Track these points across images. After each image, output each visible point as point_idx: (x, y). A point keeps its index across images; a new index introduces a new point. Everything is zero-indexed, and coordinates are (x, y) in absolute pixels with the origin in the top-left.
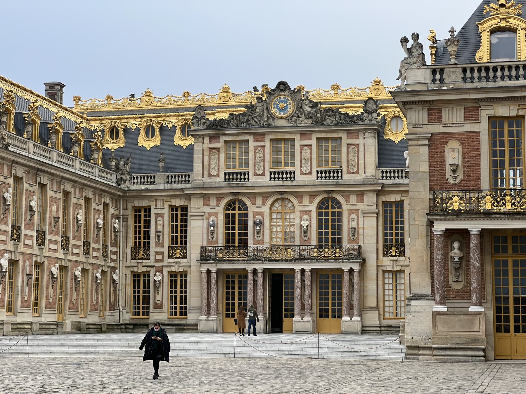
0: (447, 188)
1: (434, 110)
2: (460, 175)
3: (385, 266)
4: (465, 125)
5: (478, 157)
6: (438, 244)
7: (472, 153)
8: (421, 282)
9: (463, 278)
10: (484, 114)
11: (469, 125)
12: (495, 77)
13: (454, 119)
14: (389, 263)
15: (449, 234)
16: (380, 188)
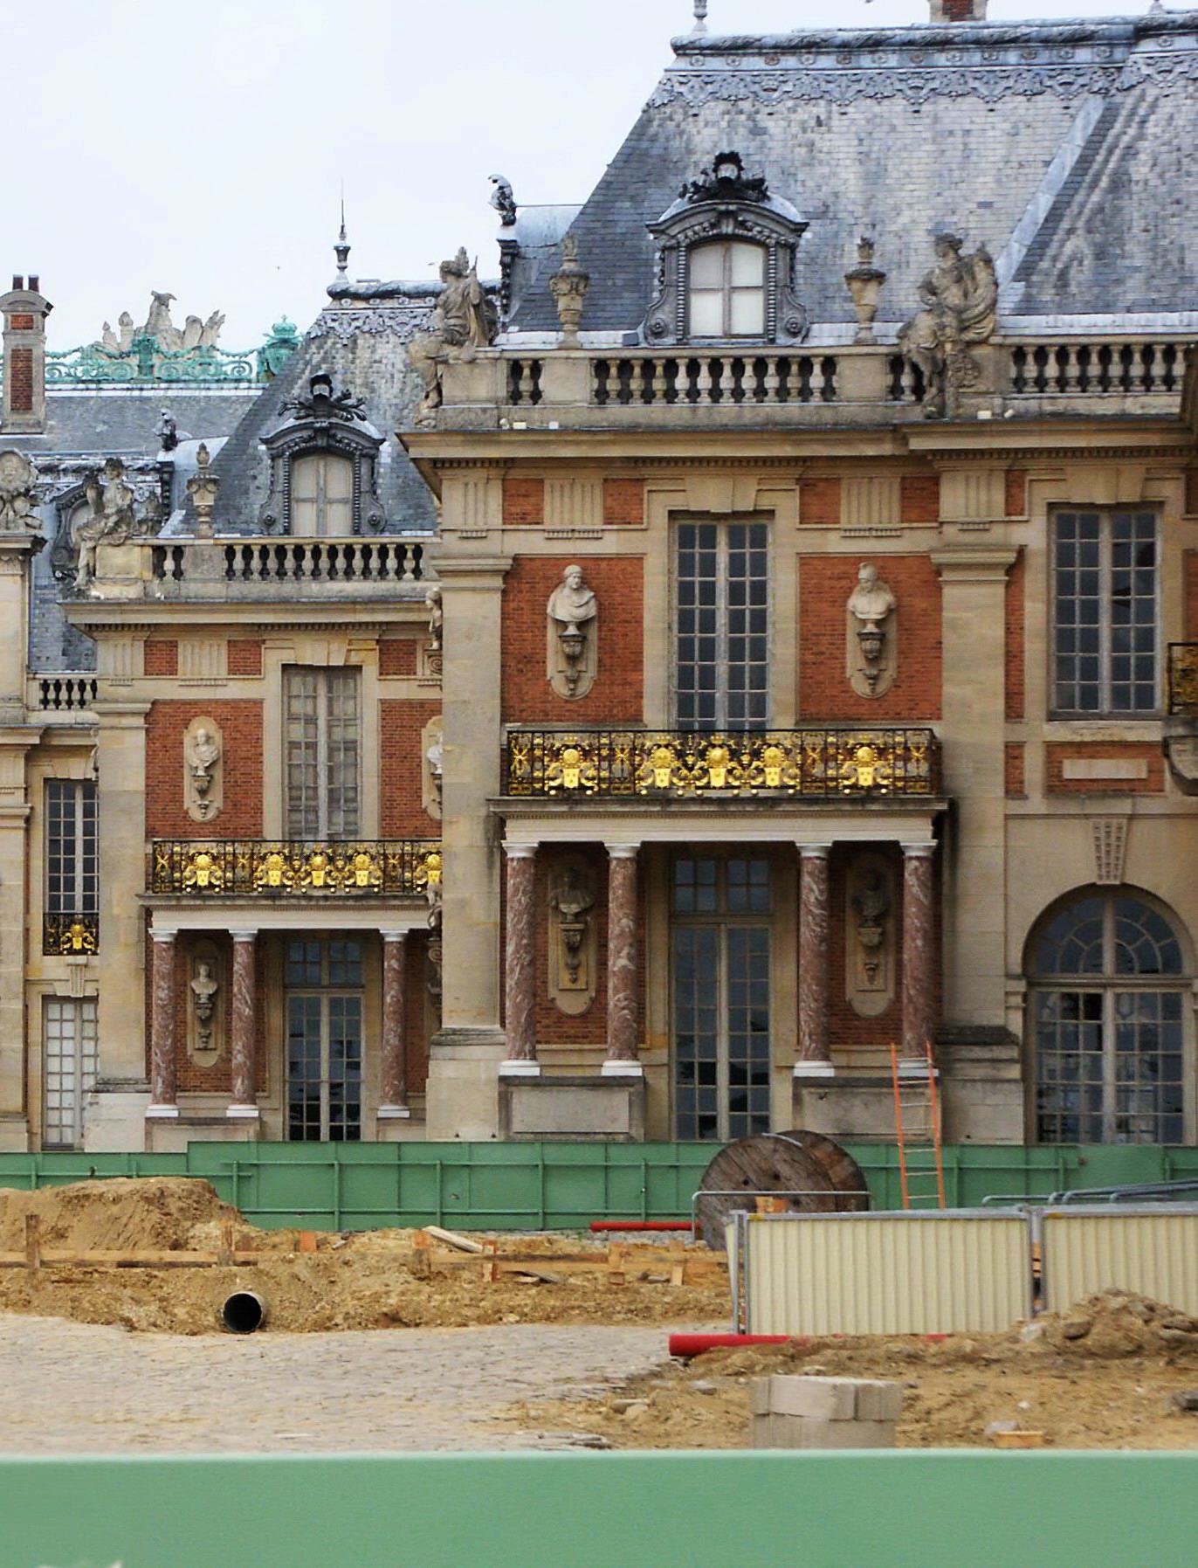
0: (184, 831)
1: (161, 647)
2: (217, 800)
3: (50, 982)
4: (231, 683)
5: (258, 758)
6: (162, 965)
7: (244, 751)
8: (123, 1048)
9: (217, 1041)
10: (273, 658)
11: (240, 683)
12: (298, 571)
13: (203, 672)
14: (62, 973)
15: (185, 938)
16: (36, 741)
